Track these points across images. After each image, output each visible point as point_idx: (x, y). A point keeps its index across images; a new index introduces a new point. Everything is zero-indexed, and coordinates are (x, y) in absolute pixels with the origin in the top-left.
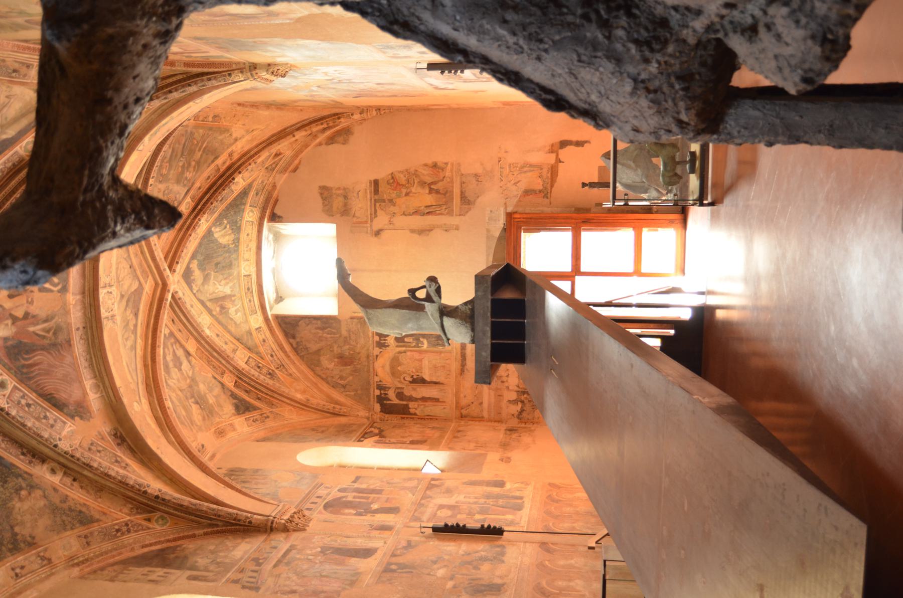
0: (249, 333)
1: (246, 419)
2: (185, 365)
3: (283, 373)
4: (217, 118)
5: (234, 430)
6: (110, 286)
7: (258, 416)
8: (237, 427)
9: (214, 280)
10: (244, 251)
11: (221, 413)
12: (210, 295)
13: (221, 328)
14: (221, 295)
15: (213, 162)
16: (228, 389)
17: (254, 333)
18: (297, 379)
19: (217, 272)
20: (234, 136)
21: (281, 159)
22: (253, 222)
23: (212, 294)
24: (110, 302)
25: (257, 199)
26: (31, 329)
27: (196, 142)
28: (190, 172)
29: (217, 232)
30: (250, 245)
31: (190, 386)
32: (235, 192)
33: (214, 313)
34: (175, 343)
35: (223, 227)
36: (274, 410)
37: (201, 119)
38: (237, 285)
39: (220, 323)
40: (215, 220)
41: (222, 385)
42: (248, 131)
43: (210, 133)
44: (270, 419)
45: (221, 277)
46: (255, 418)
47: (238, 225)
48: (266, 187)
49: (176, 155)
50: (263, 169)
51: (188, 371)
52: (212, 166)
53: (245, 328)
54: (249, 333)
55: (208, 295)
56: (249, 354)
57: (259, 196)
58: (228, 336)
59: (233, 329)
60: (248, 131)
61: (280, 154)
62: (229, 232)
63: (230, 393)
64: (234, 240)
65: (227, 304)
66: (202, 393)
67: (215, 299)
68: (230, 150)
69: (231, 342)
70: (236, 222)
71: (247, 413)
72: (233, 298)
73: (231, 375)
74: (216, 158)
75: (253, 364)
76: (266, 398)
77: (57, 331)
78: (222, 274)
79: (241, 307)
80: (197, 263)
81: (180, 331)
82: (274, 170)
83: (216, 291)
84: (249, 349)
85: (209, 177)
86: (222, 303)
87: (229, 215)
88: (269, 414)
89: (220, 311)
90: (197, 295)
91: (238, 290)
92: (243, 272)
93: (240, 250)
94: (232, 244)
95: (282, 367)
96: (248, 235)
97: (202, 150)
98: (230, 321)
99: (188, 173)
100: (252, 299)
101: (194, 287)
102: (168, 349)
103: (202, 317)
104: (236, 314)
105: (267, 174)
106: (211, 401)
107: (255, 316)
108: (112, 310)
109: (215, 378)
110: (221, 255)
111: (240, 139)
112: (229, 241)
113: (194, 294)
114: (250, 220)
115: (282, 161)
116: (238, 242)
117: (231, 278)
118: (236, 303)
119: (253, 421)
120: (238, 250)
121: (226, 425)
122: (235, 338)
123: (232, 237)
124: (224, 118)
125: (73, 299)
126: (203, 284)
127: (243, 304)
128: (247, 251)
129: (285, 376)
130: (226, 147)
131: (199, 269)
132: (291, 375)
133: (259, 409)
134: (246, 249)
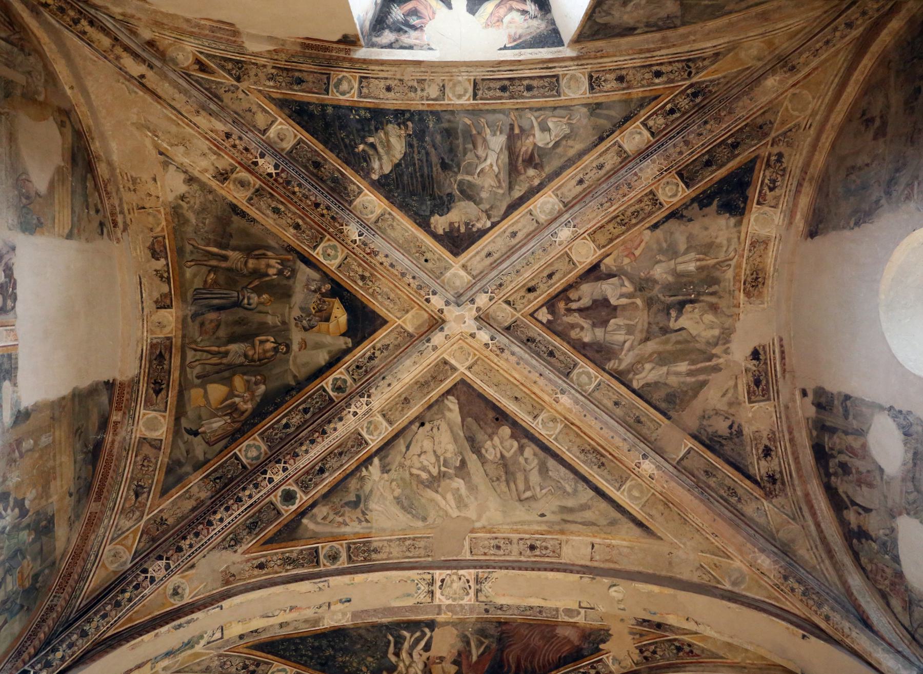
0: (595, 108)
1: (759, 203)
2: (611, 290)
3: (705, 68)
5: (766, 242)
6: (432, 583)
7: (768, 173)
8: (764, 232)
9: (472, 175)
10: (422, 98)
11: (722, 256)
12: (500, 187)
13: (569, 171)
14: (505, 157)
15: (243, 214)
16: (686, 206)
17: (600, 97)
18: (733, 47)
19: (459, 166)
21: (208, 56)
22: (361, 77)
23: (499, 182)
24: (455, 585)
25: (310, 78)
26: (474, 658)
27: (212, 276)
28: (268, 266)
29: (381, 168)
30: (410, 84)
31: (650, 303)
32: (299, 136)
33: (536, 182)
34: (569, 300)
35: (371, 152)
36: (773, 135)
38: (491, 117)
39: (557, 174)
40: (357, 172)
41: (675, 215)
42: (166, 165)
43: (188, 248)
44: (786, 155)
45: (470, 157)
46: (767, 181)
47: (368, 115)
48: (282, 64)
49: (240, 322)
50: (243, 85)
51: (624, 290)
52: (252, 212)
53: (581, 117)
54: (595, 108)
55: (501, 191)
56: (638, 123)
57: (304, 76)
58: (588, 159)
59: (578, 146)
60: (166, 160)
61: (198, 61)
62: (383, 135)
63: (695, 205)
64: (399, 125)
65: (525, 146)
66: (670, 279)
67: (510, 175)
68: (214, 184)
69: (600, 155)
70: (363, 121)
71: (750, 192)
72: (517, 131)
73: (664, 181)
74: (234, 208)
75: (661, 121)
76: (741, 129)
77: (482, 633)
78: (465, 154)
79: (536, 114)
80: (437, 216)
81: (550, 276)
82: (238, 62)
83: (495, 168)
84: (627, 119)
85: (276, 211)
86: (520, 159)
87: (347, 141)
88: (776, 150)
89: (535, 167)
90: (495, 220)
91: (501, 116)
92: (466, 101)
93: (421, 108)
94: (407, 127)
95: (690, 64)
96: (389, 89)
97: (224, 252)
98: (559, 150)
99: (272, 271)
100: (525, 83)
101: (479, 225)
102: (573, 326)
103: (537, 212)
104: (549, 130)
105: (252, 73)
106: (692, 267)
107: (563, 83)
108: (468, 581)
109: (655, 226)
110: (427, 154)
111: (186, 172)
112: (400, 136)
113: (494, 225)
114: (356, 86)
115: (217, 53)
116: (403, 112)
117: (474, 132)
118: (526, 126)
119: (771, 189)
120: (420, 113)
121: (749, 258)
122: (596, 146)
123: (392, 128)
125: (445, 613)
126: (477, 203)
127: (531, 109)
128: (422, 90)
129: (713, 67)
130: (210, 197)
131: (449, 210)
132: (717, 55)
133: (753, 161)
134: (419, 92)
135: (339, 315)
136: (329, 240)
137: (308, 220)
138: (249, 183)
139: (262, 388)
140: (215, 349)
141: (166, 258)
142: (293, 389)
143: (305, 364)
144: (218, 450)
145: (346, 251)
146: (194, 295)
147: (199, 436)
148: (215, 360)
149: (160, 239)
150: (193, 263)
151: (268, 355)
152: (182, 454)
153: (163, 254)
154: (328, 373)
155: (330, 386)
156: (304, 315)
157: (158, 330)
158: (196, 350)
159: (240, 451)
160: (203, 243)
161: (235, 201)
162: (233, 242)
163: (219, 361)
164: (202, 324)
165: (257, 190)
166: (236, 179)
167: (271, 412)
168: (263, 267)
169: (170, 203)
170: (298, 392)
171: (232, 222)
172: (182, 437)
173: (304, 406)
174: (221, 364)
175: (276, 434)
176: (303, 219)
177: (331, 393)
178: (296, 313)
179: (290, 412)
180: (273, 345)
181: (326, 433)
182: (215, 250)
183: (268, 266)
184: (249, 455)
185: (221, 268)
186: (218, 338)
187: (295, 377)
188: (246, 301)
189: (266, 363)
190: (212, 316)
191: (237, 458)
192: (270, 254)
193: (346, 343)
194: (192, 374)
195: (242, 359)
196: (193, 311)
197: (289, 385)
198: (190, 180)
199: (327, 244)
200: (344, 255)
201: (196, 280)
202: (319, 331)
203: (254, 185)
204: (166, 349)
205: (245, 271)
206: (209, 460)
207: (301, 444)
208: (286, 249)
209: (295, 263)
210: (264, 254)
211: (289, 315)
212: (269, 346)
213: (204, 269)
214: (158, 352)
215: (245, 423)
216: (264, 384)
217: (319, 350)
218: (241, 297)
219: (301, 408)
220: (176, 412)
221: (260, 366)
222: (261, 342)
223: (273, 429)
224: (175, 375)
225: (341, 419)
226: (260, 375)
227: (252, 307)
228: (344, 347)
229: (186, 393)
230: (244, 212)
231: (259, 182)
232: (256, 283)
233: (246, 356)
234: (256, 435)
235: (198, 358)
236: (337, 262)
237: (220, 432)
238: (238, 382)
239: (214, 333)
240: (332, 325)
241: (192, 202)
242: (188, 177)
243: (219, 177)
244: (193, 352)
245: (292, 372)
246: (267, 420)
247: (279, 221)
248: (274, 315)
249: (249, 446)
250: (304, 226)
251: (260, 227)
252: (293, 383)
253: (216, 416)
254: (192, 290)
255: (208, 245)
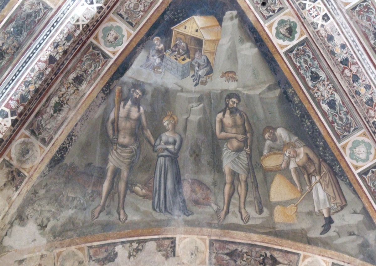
4: (101, 257)
15: (63, 150)
20: (31, 227)
27: (137, 188)
28: (128, 117)
37: (151, 246)
43: (103, 217)
49: (196, 155)
52: (60, 138)
68: (25, 188)
74: (56, 161)
85: (58, 108)
97: (109, 174)
99: (134, 114)
124: (81, 263)
130: (42, 192)
135: (195, 27)
136: (96, 38)
137: (70, 66)
138: (24, 143)
139: (281, 132)
140: (227, 188)
141: (115, 244)
142: (285, 92)
143: (255, 74)
144: (353, 196)
145: (111, 15)
146: (161, 211)
147: (333, 217)
148: (241, 189)
149: (92, 252)
150: (122, 212)
151: (239, 121)
152: (353, 241)
153: (110, 248)
154: (269, 45)
155: (286, 43)
156: (192, 73)
157: (199, 255)
158: (227, 212)
159: (357, 168)
160: (97, 199)
161: (47, 161)
162: (97, 162)
163: (243, 184)
164: (197, 203)
165: (33, 132)
166: (19, 161)
167: (313, 123)
168: (128, 125)
169: (48, 242)
170: (290, 85)
171: (73, 163)
172: (330, 238)
173: (308, 80)
174: (246, 182)
175: (341, 119)
176: (69, 73)
177: (295, 42)
178: (188, 83)
179: (314, 99)
180: (227, 115)
181: (347, 60)
182: (106, 185)
183: (128, 117)
184: (363, 156)
185: (128, 178)
186: (214, 184)
187: (270, 89)
188: (170, 147)
189: (250, 124)
190: (186, 189)
191: (366, 172)
192: (112, 116)
193: (232, 18)
194: (256, 219)
195: (243, 156)
196: (180, 213)
197: (280, 97)
198: (21, 218)
199: (102, 41)
200: (116, 18)
201: (142, 208)
202: (214, 53)
203: (26, 136)
204: (224, 248)
205: (134, 147)
206: (364, 208)
207: (357, 93)
208: (107, 95)
209: (125, 83)
210: (113, 123)
211: (190, 92)
212: (228, 120)
213: (130, 198)
214: (228, 258)
215: (322, 158)
216: (275, 129)
217: (238, 55)
218: (166, 153)
219: (310, 84)
220: (301, 242)
221: (252, 134)
222: (223, 129)
223: (332, 122)
224: (256, 239)
225: (331, 38)
226: (263, 135)
227: (178, 139)
228: (236, 21)
229: (279, 228)
230: (60, 149)
231: (23, 130)
232: (148, 133)
233: (238, 150)
234: (339, 146)
235: (237, 210)
236: (125, 27)
237: (330, 190)
238: (270, 162)
239: (208, 188)
240: (206, 36)
241: (48, 215)
242: (18, 220)
243: (17, 182)
244: (230, 215)
245: (263, 92)
246: (321, 130)
247: (72, 103)
248: (189, 112)
249: (352, 156)
250: (78, 71)
251: (79, 126)
252: (277, 92)
253: (310, 193)
254: (153, 212)
255: (100, 194)
